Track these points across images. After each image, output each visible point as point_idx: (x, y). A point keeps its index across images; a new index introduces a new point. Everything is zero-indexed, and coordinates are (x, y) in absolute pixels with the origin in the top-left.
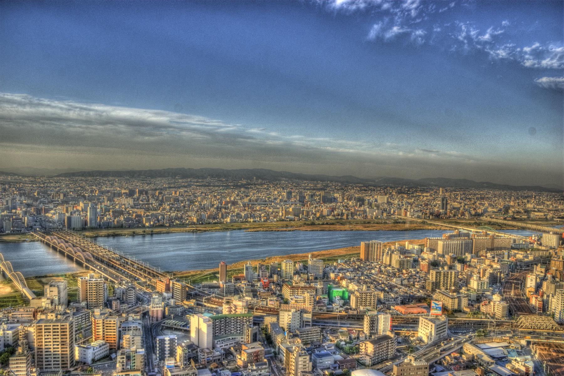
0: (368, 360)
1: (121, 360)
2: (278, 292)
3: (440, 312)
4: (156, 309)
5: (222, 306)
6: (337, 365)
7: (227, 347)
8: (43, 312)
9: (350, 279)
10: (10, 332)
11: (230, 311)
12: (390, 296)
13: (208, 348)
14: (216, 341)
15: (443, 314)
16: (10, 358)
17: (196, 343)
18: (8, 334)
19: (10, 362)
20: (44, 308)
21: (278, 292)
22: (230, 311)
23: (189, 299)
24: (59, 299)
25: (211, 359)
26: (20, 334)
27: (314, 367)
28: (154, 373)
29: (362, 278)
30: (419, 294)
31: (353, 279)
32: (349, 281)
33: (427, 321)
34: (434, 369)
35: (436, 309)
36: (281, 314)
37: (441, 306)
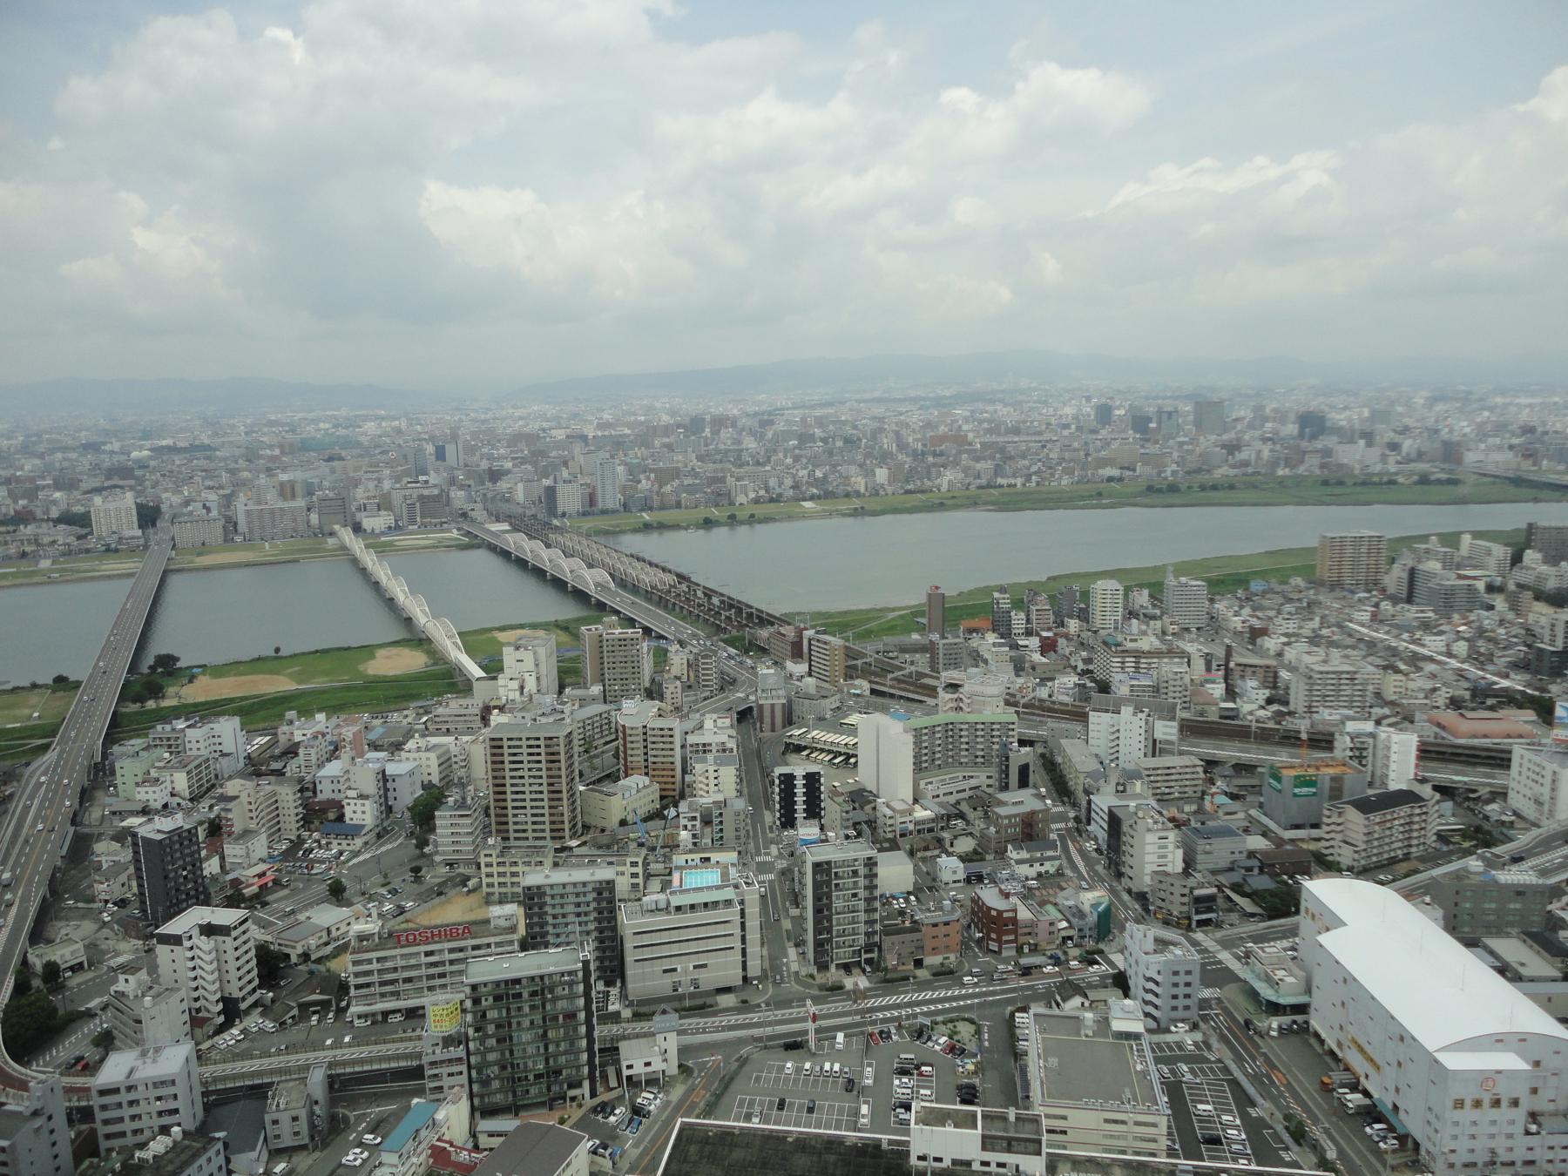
0: (1345, 856)
5: (935, 697)
6: (1255, 863)
9: (1286, 635)
10: (432, 755)
12: (1411, 685)
17: (871, 786)
23: (852, 678)
27: (1189, 863)
28: (768, 859)
29: (1325, 632)
30: (1505, 683)
31: (1294, 635)
32: (1285, 640)
36: (1093, 717)
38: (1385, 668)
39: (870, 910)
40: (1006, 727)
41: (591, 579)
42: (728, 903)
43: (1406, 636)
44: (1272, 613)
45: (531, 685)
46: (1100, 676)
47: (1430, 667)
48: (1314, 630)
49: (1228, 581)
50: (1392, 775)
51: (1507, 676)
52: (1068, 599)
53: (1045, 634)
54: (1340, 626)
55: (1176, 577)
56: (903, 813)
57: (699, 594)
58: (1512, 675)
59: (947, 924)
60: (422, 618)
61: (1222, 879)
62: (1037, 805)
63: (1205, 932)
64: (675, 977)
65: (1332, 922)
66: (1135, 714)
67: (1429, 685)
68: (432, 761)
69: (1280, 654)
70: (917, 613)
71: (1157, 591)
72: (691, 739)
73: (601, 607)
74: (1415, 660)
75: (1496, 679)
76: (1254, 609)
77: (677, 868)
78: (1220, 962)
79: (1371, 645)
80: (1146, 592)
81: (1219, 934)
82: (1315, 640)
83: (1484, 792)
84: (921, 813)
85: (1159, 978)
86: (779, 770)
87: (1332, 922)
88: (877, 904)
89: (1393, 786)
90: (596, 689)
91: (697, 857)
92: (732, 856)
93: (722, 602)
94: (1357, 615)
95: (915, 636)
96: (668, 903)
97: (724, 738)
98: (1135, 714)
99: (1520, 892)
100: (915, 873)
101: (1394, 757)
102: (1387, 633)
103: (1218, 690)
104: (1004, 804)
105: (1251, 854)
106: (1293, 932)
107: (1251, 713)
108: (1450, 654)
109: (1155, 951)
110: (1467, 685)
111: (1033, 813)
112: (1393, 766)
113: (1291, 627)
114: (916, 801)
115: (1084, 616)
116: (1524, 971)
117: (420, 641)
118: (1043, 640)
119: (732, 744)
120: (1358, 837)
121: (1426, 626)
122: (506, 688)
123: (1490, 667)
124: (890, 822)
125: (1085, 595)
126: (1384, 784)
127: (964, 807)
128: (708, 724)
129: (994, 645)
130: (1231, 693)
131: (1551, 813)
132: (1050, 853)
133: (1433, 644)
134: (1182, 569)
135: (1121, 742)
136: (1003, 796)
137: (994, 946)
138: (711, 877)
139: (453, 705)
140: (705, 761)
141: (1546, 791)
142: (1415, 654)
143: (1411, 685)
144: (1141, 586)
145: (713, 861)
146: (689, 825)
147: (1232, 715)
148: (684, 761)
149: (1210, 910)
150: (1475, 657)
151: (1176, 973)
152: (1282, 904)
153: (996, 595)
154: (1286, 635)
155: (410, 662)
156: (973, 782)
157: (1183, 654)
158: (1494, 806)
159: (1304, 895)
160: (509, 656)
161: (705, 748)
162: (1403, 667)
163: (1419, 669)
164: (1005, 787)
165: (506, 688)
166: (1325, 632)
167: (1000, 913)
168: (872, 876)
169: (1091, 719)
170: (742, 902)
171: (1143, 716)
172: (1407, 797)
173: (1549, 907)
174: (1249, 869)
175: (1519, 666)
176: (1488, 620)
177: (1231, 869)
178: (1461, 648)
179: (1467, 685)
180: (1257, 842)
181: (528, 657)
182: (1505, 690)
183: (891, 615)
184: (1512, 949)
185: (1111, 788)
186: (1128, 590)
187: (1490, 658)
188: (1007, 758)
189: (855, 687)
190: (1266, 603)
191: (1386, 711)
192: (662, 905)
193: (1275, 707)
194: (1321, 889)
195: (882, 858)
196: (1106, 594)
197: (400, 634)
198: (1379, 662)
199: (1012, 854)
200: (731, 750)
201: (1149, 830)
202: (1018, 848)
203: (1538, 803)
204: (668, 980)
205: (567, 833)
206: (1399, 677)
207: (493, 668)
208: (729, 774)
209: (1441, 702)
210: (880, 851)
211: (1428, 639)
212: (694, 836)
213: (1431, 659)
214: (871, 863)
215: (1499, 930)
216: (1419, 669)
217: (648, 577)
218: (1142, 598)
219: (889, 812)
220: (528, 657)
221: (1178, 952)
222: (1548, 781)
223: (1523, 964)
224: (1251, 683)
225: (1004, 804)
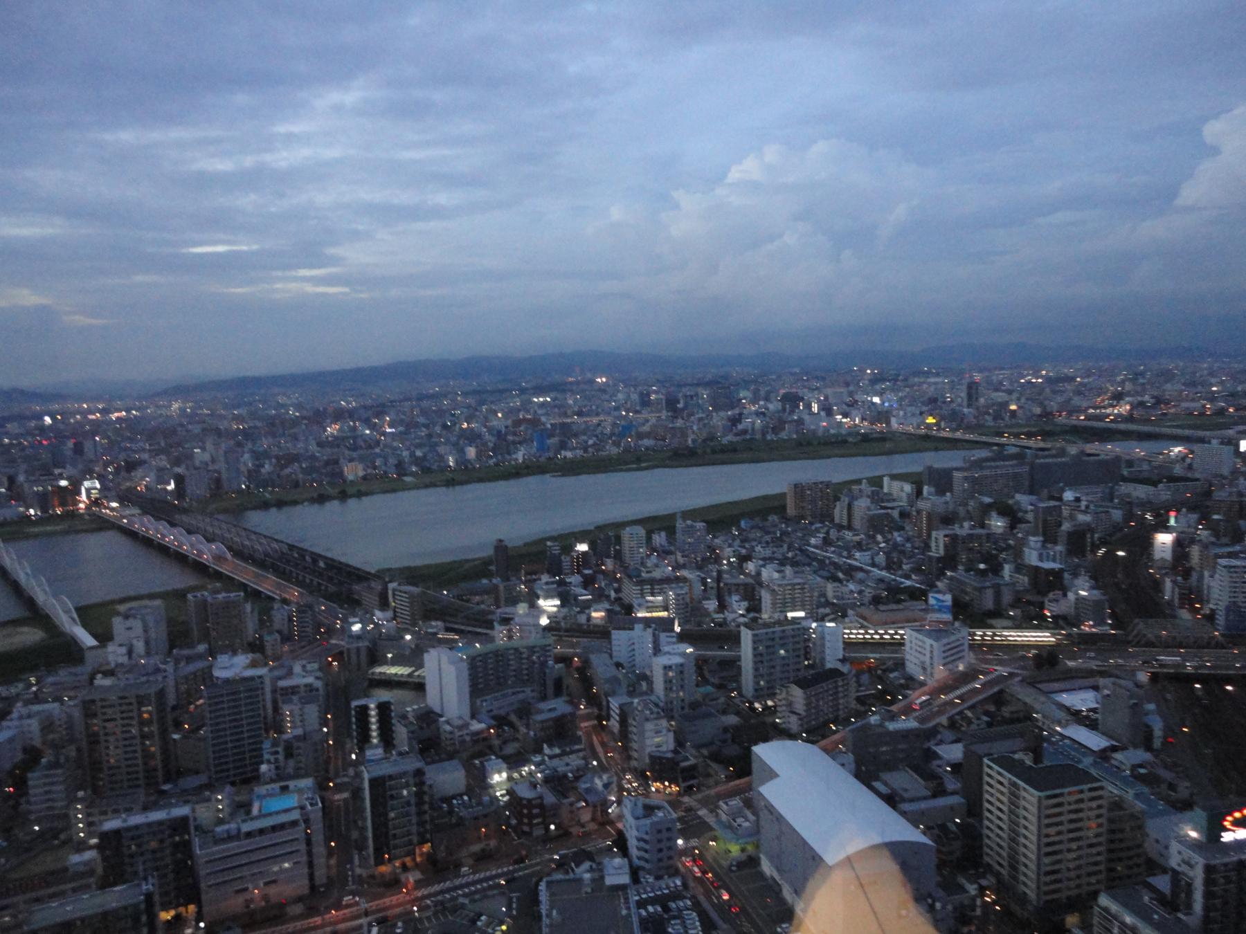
0: (794, 723)
1: (272, 758)
2: (613, 594)
3: (948, 617)
4: (355, 645)
5: (492, 628)
6: (729, 736)
7: (502, 712)
8: (109, 673)
9: (764, 559)
11: (510, 638)
13: (460, 718)
14: (478, 702)
15: (956, 618)
16: (30, 775)
17: (437, 709)
18: (29, 725)
19: (30, 783)
20: (113, 665)
21: (613, 594)
22: (510, 638)
24: (147, 643)
25: (468, 738)
26: (58, 723)
27: (680, 743)
28: (346, 780)
30: (908, 583)
32: (761, 562)
33: (920, 637)
34: (939, 737)
35: (940, 610)
36: (616, 634)
37: (949, 603)
38: (828, 579)
39: (420, 813)
40: (544, 648)
41: (207, 552)
42: (294, 824)
43: (845, 554)
44: (754, 544)
45: (140, 646)
46: (626, 601)
47: (860, 575)
48: (783, 555)
49: (720, 519)
50: (828, 658)
51: (908, 577)
52: (606, 539)
53: (587, 572)
54: (801, 550)
55: (684, 520)
56: (460, 728)
57: (308, 558)
59: (485, 816)
60: (41, 595)
61: (705, 752)
62: (568, 709)
63: (690, 796)
64: (247, 896)
65: (772, 775)
66: (645, 629)
67: (859, 588)
68: (34, 725)
69: (759, 574)
70: (486, 562)
71: (671, 531)
72: (283, 683)
73: (218, 576)
74: (850, 571)
76: (742, 541)
77: (258, 797)
78: (700, 817)
79: (822, 562)
80: (663, 534)
81: (699, 796)
82: (783, 562)
83: (890, 663)
84: (476, 726)
85: (647, 837)
86: (354, 704)
87: (772, 775)
88: (426, 807)
89: (829, 666)
90: (202, 648)
91: (277, 786)
92: (307, 782)
93: (326, 564)
94: (813, 541)
95: (485, 581)
96: (239, 830)
97: (310, 680)
98: (645, 629)
99: (905, 735)
100: (467, 776)
101: (828, 644)
102: (833, 552)
103: (711, 605)
104: (541, 712)
105: (726, 730)
106: (749, 788)
107: (734, 620)
108: (874, 565)
109: (645, 817)
110: (882, 586)
111: (563, 716)
112: (827, 651)
113: (768, 553)
114: (473, 716)
115: (618, 556)
116: (906, 795)
117: (35, 615)
118: (584, 576)
119: (318, 684)
120: (800, 706)
121: (859, 546)
122: (115, 653)
124: (449, 736)
125: (618, 539)
126: (823, 665)
127: (513, 718)
128: (297, 669)
129: (547, 583)
130: (722, 607)
131: (932, 674)
132: (577, 747)
133: (860, 558)
134: (687, 514)
135: (636, 653)
136: (542, 706)
137: (526, 829)
138: (292, 801)
139: (63, 675)
140: (290, 701)
141: (927, 659)
142: (850, 565)
143: (844, 589)
144: (660, 530)
145: (291, 787)
146: (272, 758)
147: (724, 623)
148: (275, 702)
149: (694, 777)
150: (888, 568)
151: (659, 831)
152: (743, 766)
153: (549, 543)
154: (764, 559)
155: (30, 636)
156: (521, 696)
157: (684, 580)
158: (895, 674)
159: (754, 757)
160: (118, 624)
161: (294, 690)
162: (841, 575)
163: (852, 577)
164: (544, 698)
165: (115, 653)
166: (790, 555)
167: (529, 801)
168: (420, 784)
169: (613, 637)
170: (307, 821)
171: (650, 631)
172: (835, 673)
173: (926, 745)
174: (724, 741)
175: (917, 570)
176: (898, 537)
177: (712, 743)
178: (881, 558)
180: (732, 720)
181: (137, 625)
183: (467, 566)
184: (904, 780)
185: (624, 689)
186: (649, 534)
188: (545, 674)
189: (432, 627)
190: (752, 536)
191: (827, 610)
192: (234, 833)
193: (752, 615)
194: (763, 751)
195: (427, 769)
196: (632, 538)
197: (16, 612)
198: (825, 574)
199: (547, 750)
200: (317, 690)
201: (647, 720)
202: (551, 746)
203: (924, 669)
204: (240, 899)
205: (160, 780)
206: (836, 584)
207: (104, 637)
208: (312, 711)
209: (866, 600)
210: (427, 764)
211: (858, 555)
212: (277, 768)
213: (861, 569)
214: (419, 773)
215: (890, 766)
216: (852, 577)
217: (259, 547)
218: (659, 539)
219: (448, 728)
220: (137, 625)
221: (661, 814)
223: (906, 790)
224: (735, 598)
225: (541, 712)
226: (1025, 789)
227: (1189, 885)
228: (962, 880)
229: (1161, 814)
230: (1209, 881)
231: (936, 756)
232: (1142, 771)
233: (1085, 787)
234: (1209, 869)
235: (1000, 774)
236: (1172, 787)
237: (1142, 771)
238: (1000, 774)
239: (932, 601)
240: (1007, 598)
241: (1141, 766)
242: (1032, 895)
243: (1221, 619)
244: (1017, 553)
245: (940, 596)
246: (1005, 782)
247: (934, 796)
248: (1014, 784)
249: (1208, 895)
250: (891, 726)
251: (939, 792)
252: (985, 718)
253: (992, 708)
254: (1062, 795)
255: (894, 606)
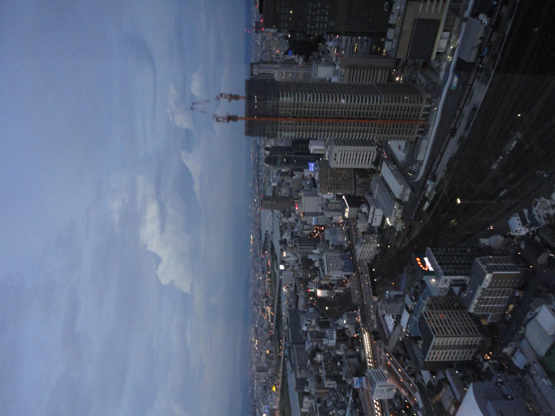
3: (364, 379)
15: (364, 375)
30: (351, 398)
33: (375, 392)
34: (421, 382)
35: (361, 383)
37: (357, 378)
51: (348, 399)
58: (347, 395)
75: (350, 401)
110: (354, 411)
123: (346, 403)
131: (392, 386)
141: (385, 388)
150: (344, 408)
173: (426, 388)
175: (344, 394)
176: (330, 404)
179: (354, 411)
182: (353, 398)
187: (343, 403)
203: (390, 390)
222: (382, 388)
223: (450, 397)
226: (434, 343)
227: (454, 280)
228: (484, 370)
229: (428, 290)
230: (450, 274)
231: (430, 383)
232: (413, 298)
233: (426, 319)
234: (445, 274)
235: (430, 354)
236: (417, 287)
237: (413, 298)
238: (430, 354)
239: (358, 387)
240: (351, 352)
241: (412, 299)
242: (480, 339)
243: (348, 273)
244: (331, 348)
245: (355, 383)
246: (433, 352)
247: (449, 383)
248: (433, 348)
249: (456, 274)
250: (421, 405)
251: (446, 380)
252: (407, 361)
253: (402, 358)
254: (432, 328)
255: (363, 406)
